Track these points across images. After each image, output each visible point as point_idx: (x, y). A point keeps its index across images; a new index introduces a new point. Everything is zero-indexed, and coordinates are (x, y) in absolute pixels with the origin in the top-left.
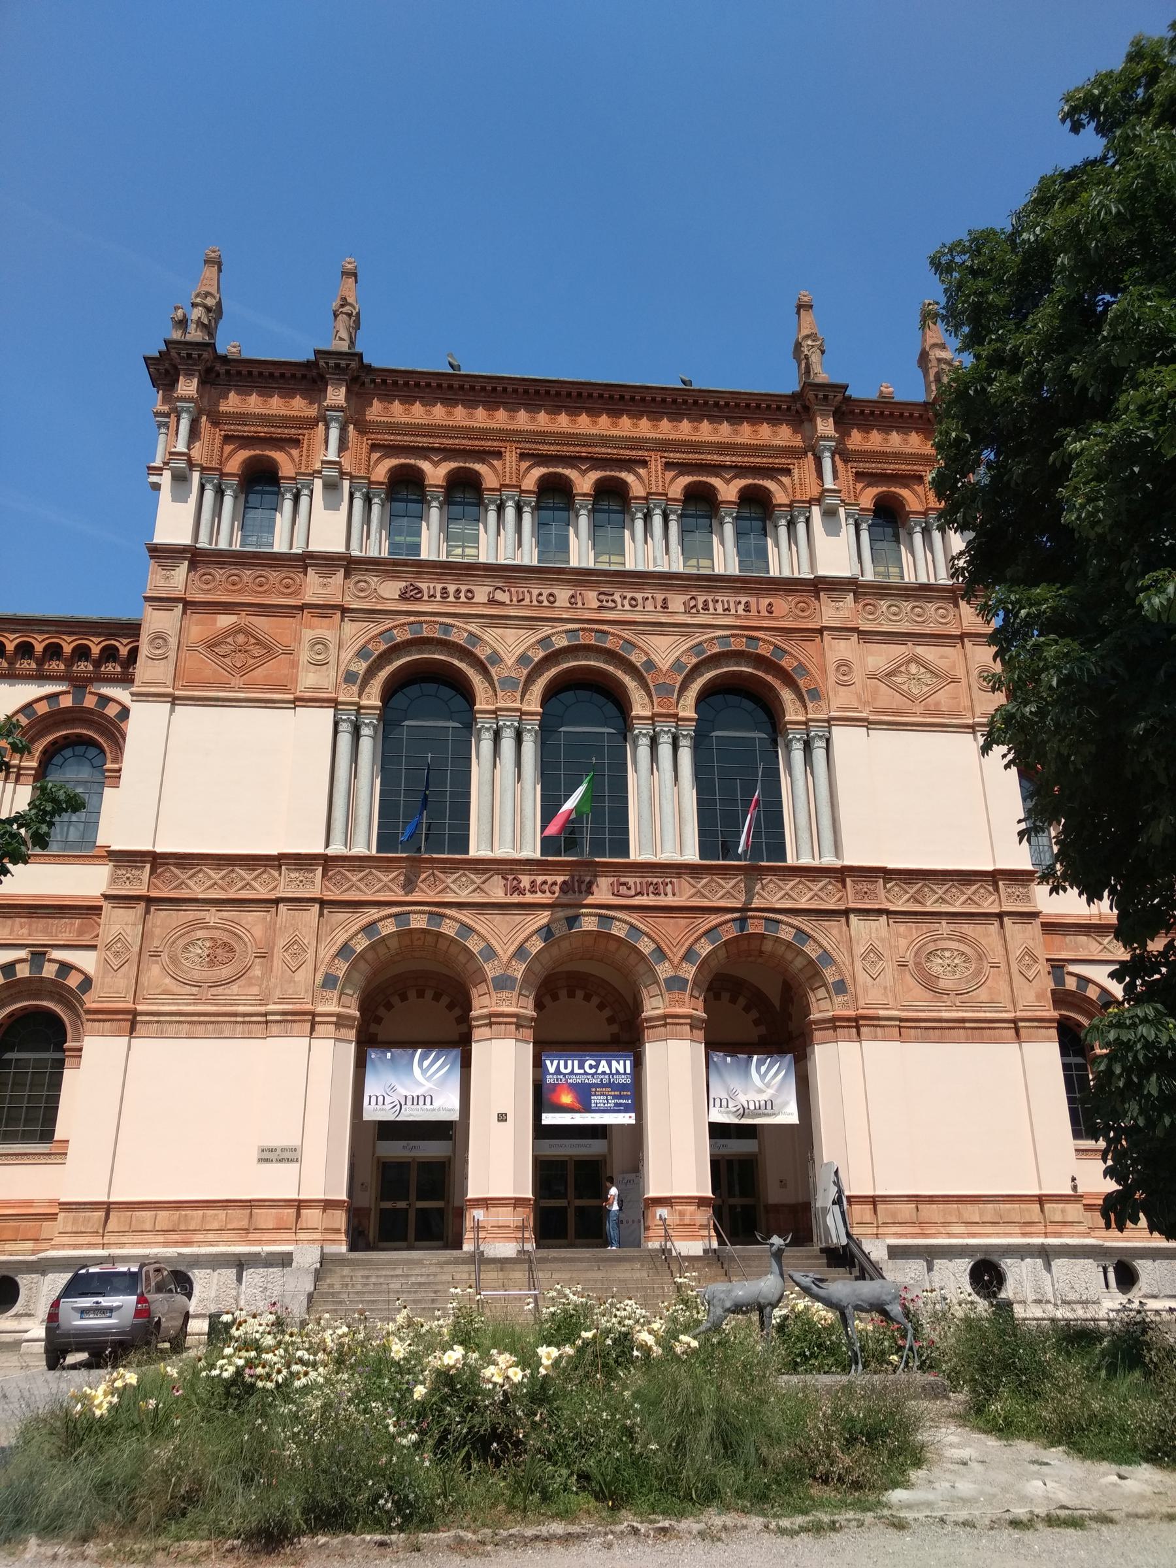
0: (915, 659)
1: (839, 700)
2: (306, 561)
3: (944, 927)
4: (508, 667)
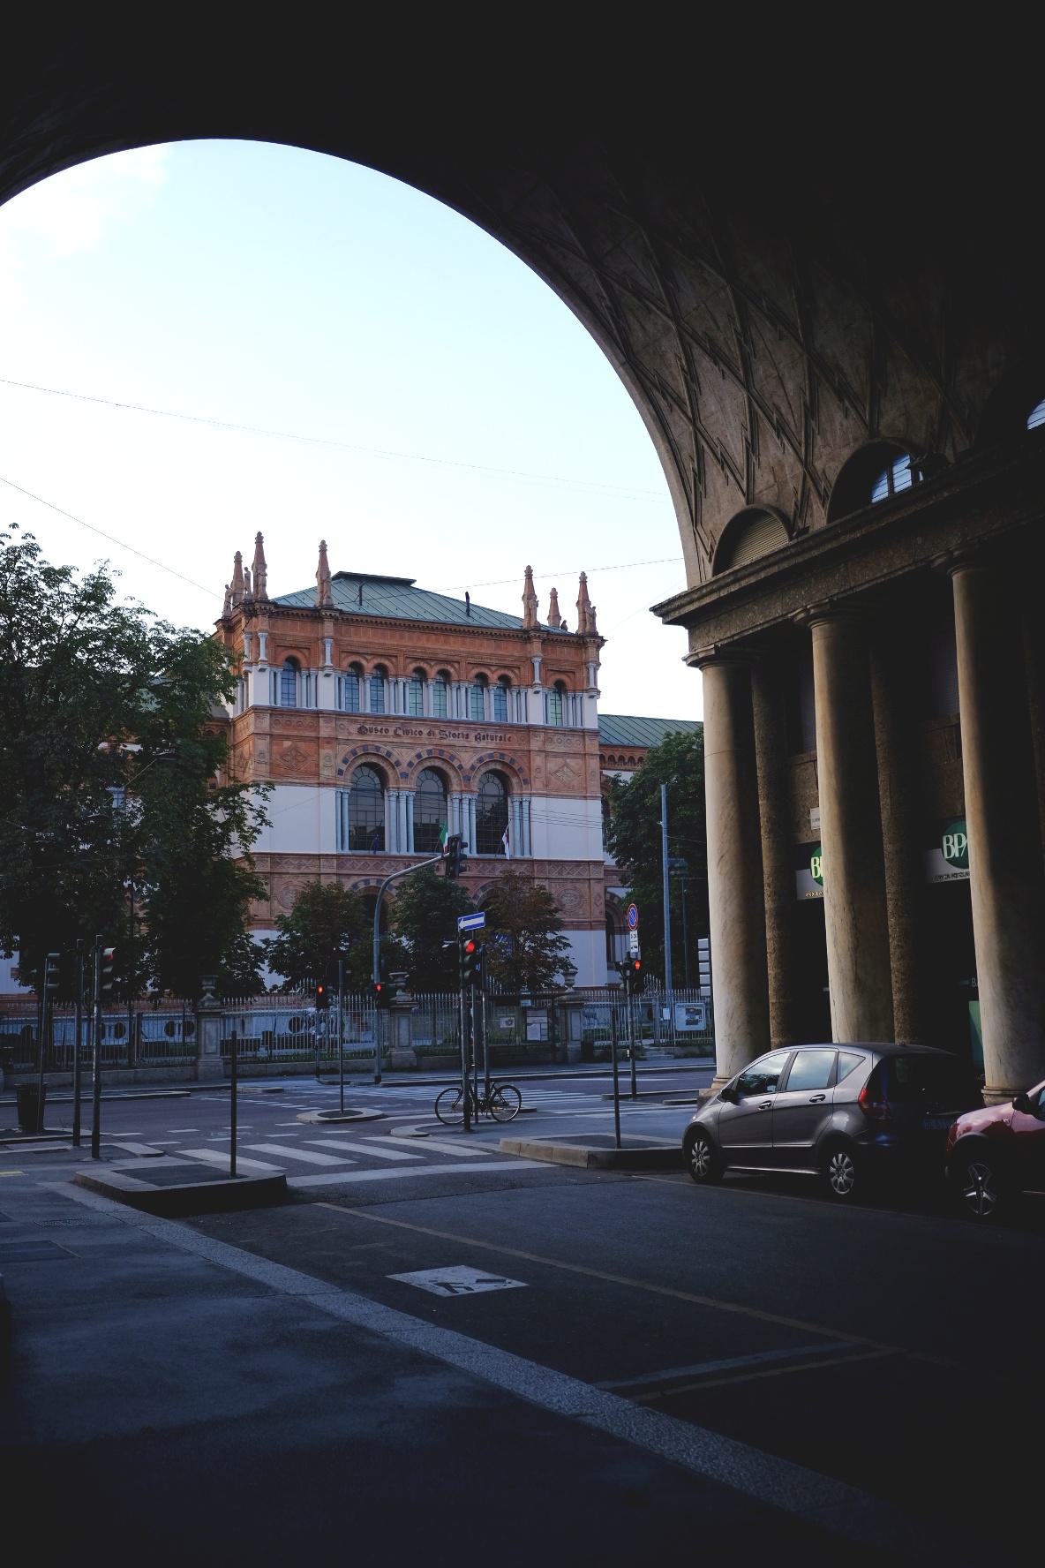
0: (566, 765)
1: (537, 785)
2: (318, 714)
3: (569, 885)
4: (404, 767)
